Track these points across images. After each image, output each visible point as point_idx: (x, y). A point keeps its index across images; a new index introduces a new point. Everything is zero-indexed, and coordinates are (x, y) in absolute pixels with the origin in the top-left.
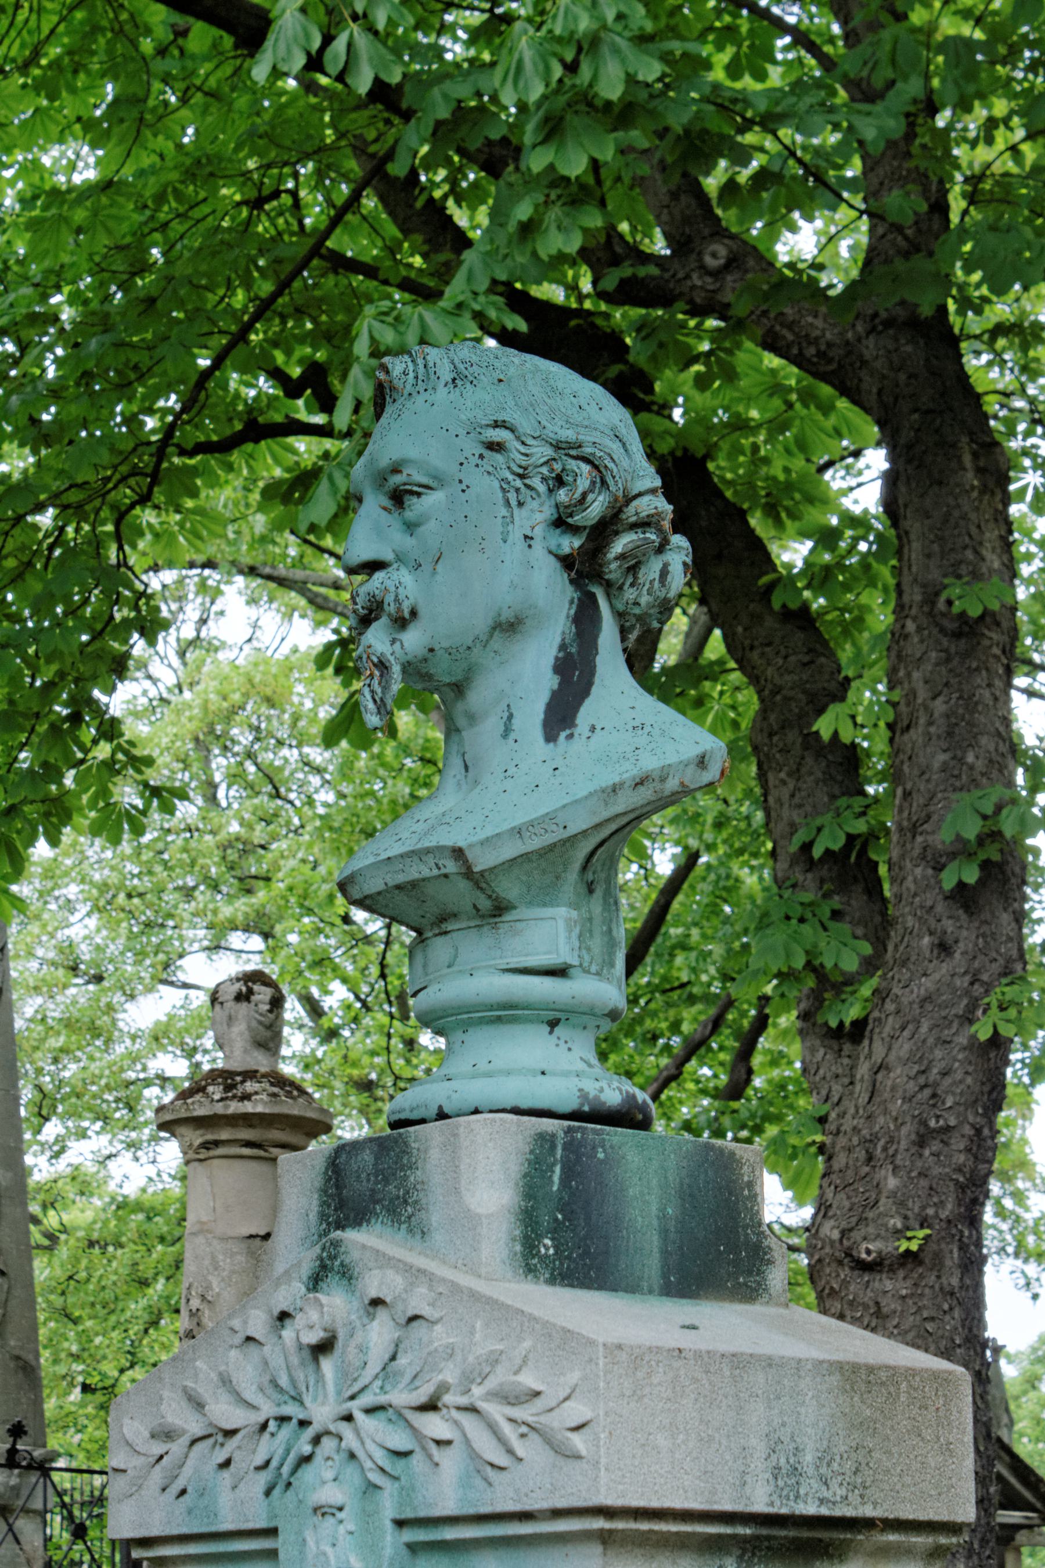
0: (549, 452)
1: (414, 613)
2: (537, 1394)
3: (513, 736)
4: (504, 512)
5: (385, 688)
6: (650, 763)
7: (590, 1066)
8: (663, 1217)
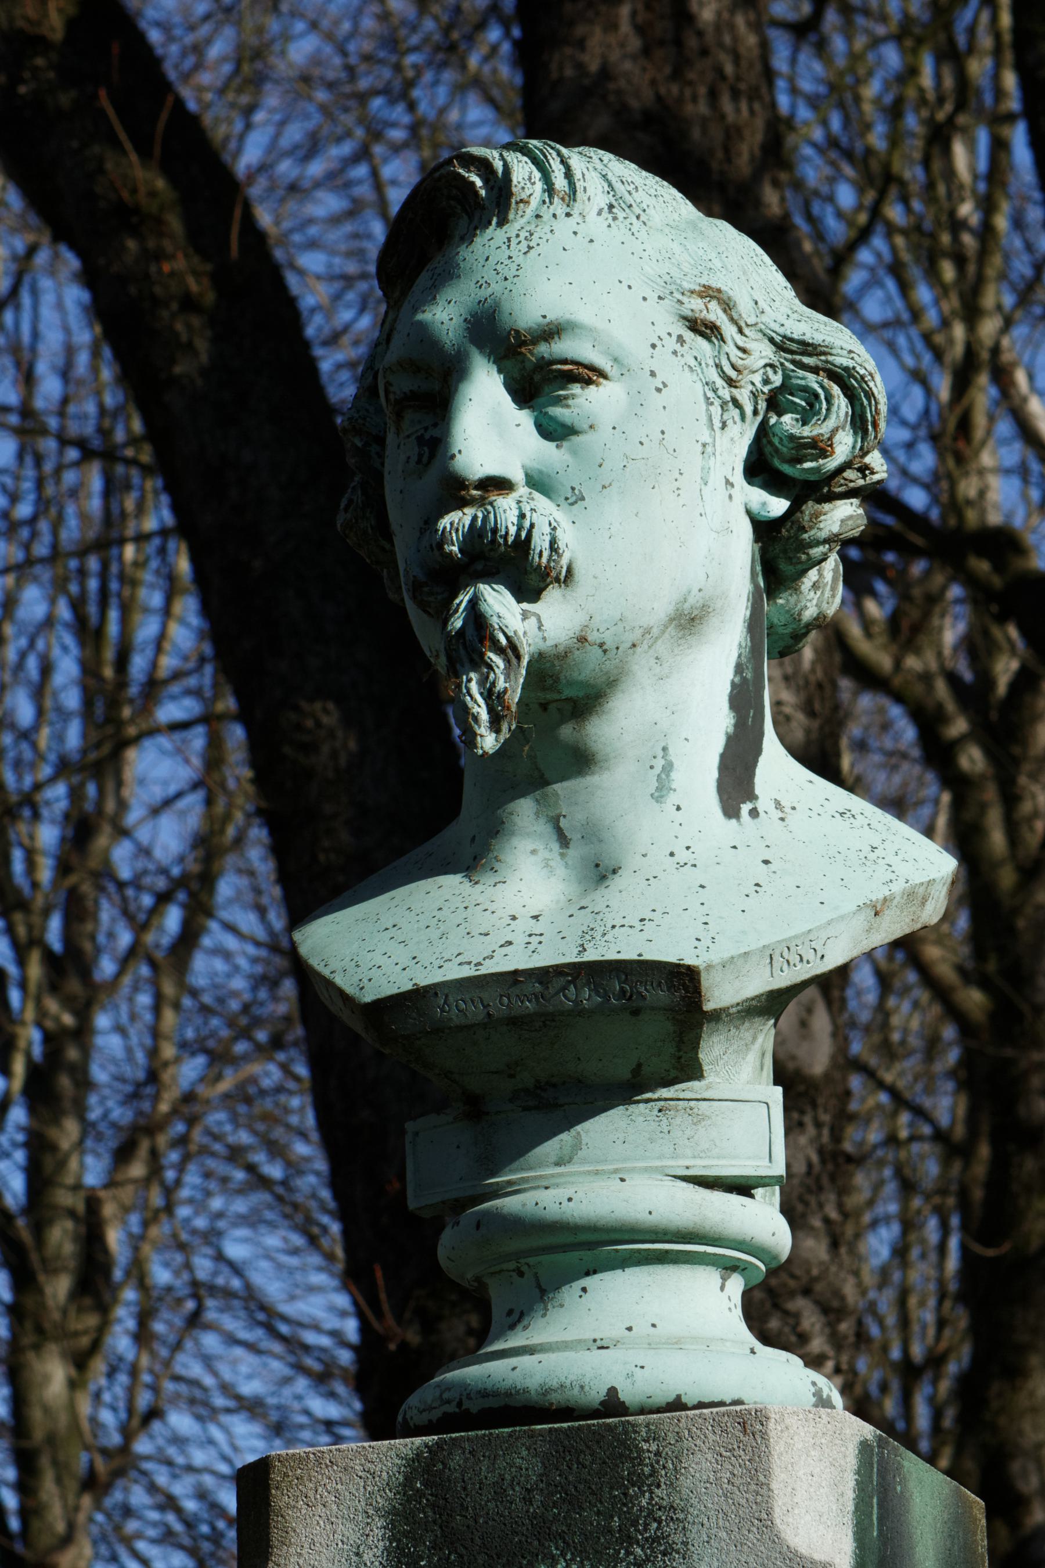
3: (672, 799)
4: (705, 437)
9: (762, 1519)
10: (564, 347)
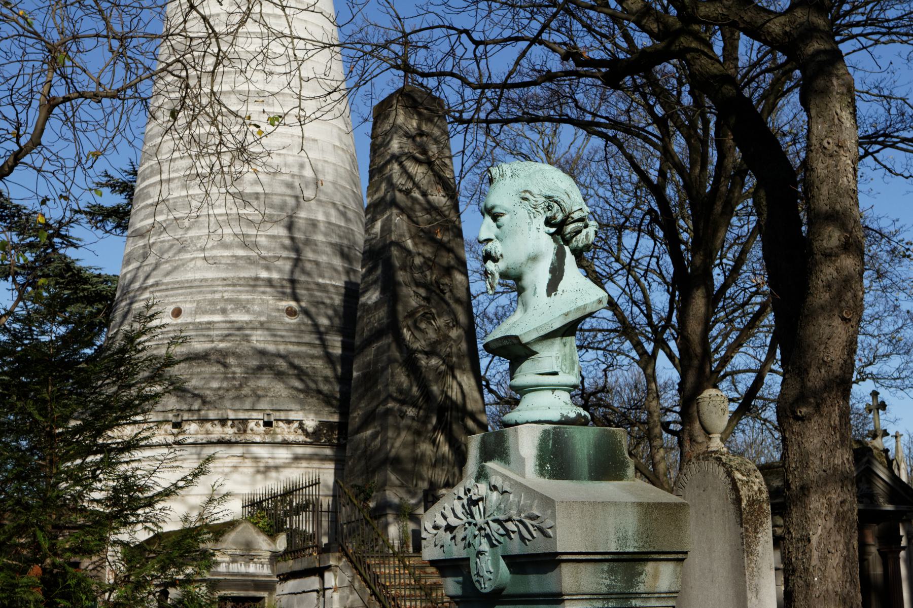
0: (544, 199)
1: (501, 255)
2: (538, 517)
5: (494, 281)
6: (580, 303)
7: (567, 404)
8: (589, 455)
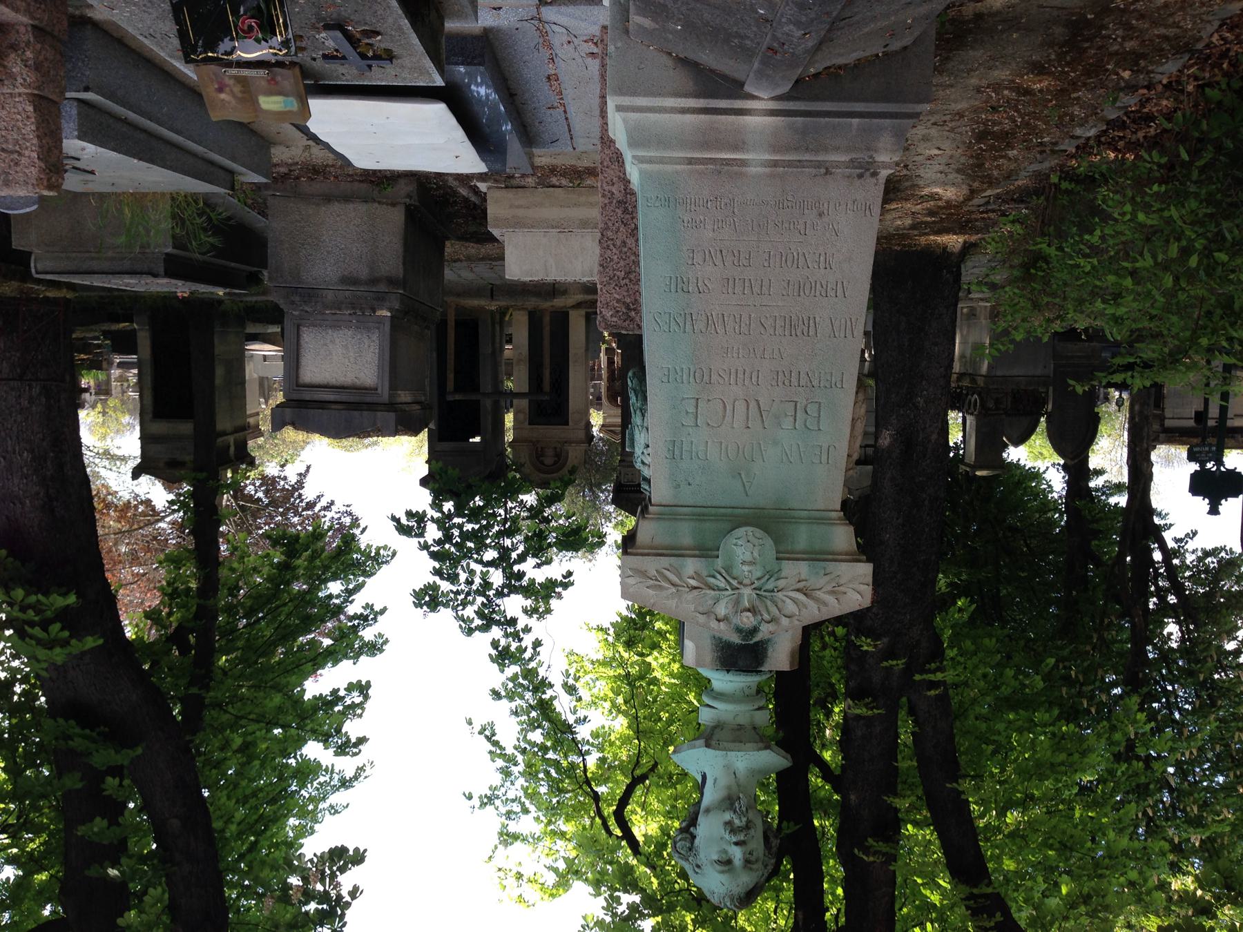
9: (697, 647)
10: (719, 868)
